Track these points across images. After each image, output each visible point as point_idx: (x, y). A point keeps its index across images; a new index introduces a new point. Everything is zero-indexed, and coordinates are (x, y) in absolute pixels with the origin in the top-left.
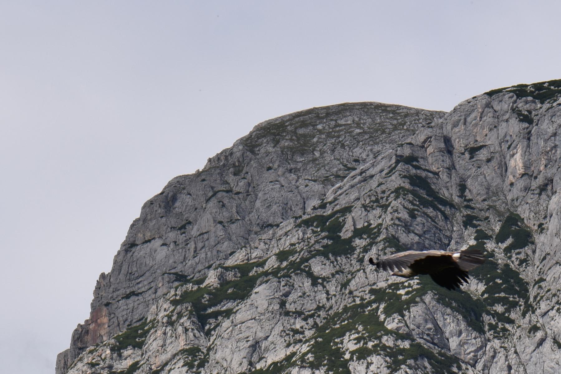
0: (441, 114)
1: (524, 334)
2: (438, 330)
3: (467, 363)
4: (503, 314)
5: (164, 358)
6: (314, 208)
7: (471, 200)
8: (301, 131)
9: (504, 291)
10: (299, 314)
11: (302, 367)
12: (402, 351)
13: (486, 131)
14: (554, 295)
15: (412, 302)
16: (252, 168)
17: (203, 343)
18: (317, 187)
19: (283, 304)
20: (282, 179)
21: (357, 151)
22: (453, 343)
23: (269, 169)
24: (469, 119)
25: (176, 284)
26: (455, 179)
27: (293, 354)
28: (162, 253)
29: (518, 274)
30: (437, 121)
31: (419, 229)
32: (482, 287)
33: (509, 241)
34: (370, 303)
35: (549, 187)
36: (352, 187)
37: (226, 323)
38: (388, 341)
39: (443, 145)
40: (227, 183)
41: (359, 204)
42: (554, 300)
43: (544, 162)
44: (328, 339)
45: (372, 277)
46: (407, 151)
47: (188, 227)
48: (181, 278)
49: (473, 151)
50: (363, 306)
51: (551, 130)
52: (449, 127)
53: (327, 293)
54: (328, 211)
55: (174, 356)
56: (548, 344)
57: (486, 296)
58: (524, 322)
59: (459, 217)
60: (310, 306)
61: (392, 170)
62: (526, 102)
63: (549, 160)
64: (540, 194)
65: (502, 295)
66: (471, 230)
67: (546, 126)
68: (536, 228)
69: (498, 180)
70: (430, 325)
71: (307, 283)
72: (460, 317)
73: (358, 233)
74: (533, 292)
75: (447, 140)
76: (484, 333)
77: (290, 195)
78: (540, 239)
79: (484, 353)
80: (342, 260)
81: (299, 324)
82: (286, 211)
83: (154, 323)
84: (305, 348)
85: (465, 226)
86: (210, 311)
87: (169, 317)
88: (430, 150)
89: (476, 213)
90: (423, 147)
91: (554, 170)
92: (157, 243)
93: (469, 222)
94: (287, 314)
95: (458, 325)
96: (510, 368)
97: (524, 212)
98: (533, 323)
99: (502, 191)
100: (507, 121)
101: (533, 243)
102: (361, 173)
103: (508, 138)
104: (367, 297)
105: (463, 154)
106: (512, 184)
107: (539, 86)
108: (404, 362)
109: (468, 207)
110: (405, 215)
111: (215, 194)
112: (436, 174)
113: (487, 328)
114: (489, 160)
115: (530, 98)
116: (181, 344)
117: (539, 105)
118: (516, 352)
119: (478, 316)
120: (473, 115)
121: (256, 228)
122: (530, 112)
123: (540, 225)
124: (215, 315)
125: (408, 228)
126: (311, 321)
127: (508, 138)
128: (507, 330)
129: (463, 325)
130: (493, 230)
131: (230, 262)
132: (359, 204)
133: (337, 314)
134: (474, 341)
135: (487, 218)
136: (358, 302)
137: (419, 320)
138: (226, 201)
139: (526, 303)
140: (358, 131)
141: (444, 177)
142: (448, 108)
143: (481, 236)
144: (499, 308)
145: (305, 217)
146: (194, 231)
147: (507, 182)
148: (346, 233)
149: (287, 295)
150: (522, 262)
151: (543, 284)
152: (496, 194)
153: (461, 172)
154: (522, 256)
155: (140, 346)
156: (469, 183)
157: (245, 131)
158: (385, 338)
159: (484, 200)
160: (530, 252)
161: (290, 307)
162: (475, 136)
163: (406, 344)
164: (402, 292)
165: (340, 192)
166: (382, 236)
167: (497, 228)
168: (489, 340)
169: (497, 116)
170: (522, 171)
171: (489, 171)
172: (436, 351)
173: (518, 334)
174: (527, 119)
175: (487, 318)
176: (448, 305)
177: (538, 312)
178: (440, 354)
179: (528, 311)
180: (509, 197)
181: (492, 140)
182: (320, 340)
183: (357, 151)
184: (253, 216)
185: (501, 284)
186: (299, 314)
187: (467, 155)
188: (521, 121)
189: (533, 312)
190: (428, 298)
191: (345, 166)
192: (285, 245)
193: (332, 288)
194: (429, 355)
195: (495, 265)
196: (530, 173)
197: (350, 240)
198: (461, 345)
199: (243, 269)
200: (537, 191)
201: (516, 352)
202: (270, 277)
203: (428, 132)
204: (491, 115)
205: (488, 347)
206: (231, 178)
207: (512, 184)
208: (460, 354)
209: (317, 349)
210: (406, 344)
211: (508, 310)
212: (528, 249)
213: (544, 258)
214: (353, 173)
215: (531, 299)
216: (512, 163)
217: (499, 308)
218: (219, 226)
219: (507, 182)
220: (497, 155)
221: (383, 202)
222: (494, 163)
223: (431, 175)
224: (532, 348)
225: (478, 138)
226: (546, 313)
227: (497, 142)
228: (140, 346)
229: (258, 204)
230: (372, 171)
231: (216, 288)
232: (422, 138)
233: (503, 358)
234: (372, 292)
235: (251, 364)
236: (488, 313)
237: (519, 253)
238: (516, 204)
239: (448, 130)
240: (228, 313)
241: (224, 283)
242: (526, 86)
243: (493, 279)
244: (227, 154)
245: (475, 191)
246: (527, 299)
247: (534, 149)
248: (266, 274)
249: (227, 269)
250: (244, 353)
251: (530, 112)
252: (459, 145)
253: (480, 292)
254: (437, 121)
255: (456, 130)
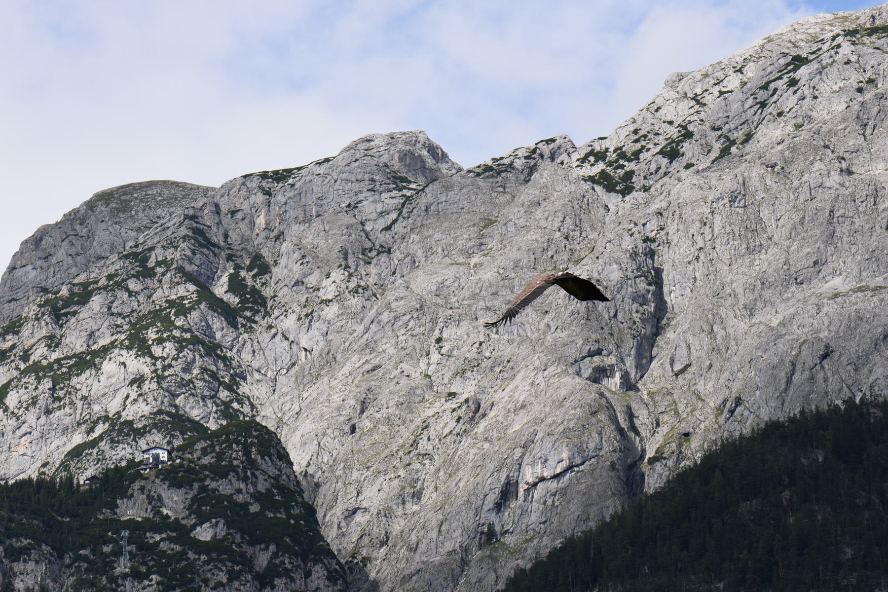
0: (213, 189)
1: (264, 330)
2: (209, 326)
3: (227, 348)
4: (251, 317)
5: (32, 341)
6: (131, 247)
7: (231, 244)
8: (123, 198)
9: (251, 302)
10: (119, 314)
11: (121, 349)
12: (185, 340)
13: (242, 200)
14: (283, 306)
15: (192, 308)
16: (91, 221)
17: (58, 332)
18: (133, 234)
19: (109, 308)
20: (110, 228)
21: (159, 212)
22: (218, 335)
23: (103, 221)
24: (231, 193)
25: (41, 294)
26: (221, 231)
27: (116, 340)
28: (33, 274)
29: (261, 292)
30: (210, 193)
31: (198, 262)
32: (237, 300)
33: (255, 271)
34: (165, 309)
35: (281, 237)
36: (156, 234)
37: (73, 320)
38: (177, 333)
39: (214, 209)
40: (75, 230)
41: (159, 245)
42: (283, 309)
43: (278, 221)
44: (138, 331)
45: (167, 292)
46: (191, 212)
47: (50, 258)
48: (45, 290)
49: (233, 213)
50: (161, 310)
51: (283, 201)
52: (218, 197)
53: (138, 302)
54: (140, 249)
55: (39, 340)
56: (279, 336)
57: (240, 305)
58: (264, 323)
59: (223, 255)
60: (127, 310)
61: (181, 224)
62: (268, 183)
63: (282, 220)
64: (275, 241)
65: (250, 305)
66: (231, 263)
67: (280, 198)
68: (272, 263)
69: (249, 232)
70: (203, 324)
71: (126, 295)
72: (223, 319)
73: (159, 264)
74: (270, 303)
75: (217, 206)
76: (238, 329)
77: (116, 238)
78: (275, 270)
79: (238, 342)
80: (148, 281)
81: (119, 321)
82: (113, 248)
83: (27, 319)
84: (123, 337)
85: (227, 261)
86: (63, 311)
87: (36, 315)
88: (206, 211)
89: (234, 252)
90: (201, 209)
91: (285, 226)
92: (30, 267)
93: (229, 258)
94: (112, 314)
95: (221, 323)
96: (254, 352)
97: (265, 252)
98: (269, 324)
99: (251, 239)
100: (255, 194)
101: (270, 272)
102: (161, 226)
103: (256, 205)
104: (164, 305)
105: (227, 214)
106: (258, 235)
107: (276, 173)
108: (186, 347)
109: (229, 248)
110: (188, 253)
111: (67, 236)
112: (209, 227)
113: (240, 326)
114: (243, 219)
115: (270, 180)
116: (44, 332)
117: (276, 185)
118: (258, 342)
119: (235, 318)
120: (233, 190)
121: (93, 259)
122: (270, 189)
123: (275, 261)
124: (66, 314)
125: (190, 261)
126: (127, 319)
127: (256, 205)
128: (253, 328)
129: (225, 324)
130: (245, 264)
131: (76, 281)
132: (159, 245)
133: (144, 315)
134: (231, 334)
135: (241, 256)
136: (158, 307)
137: (197, 320)
138: (74, 242)
139: (265, 310)
140: (160, 198)
141: (214, 229)
142: (217, 185)
143: (237, 267)
144: (248, 314)
145: (125, 253)
146: (53, 260)
147: (255, 233)
148: (151, 263)
149: (112, 302)
150: (263, 284)
151: (276, 299)
152: (247, 241)
153: (226, 226)
154: (263, 281)
155: (17, 333)
156: (230, 233)
157: (88, 196)
158: (174, 331)
159: (240, 244)
160: (268, 278)
161: (114, 310)
162: (235, 203)
163: (188, 336)
164: (186, 302)
165: (147, 237)
166: (174, 266)
167: (248, 263)
168: (241, 334)
169: (249, 191)
170: (264, 226)
171: (243, 226)
172: (207, 340)
173: (259, 330)
174: (268, 193)
175: (240, 320)
176: (215, 311)
177: (273, 316)
178: (209, 342)
179: (266, 315)
180: (256, 243)
181: (246, 206)
182: (133, 331)
183: (159, 212)
184: (92, 251)
185: (250, 298)
186: (119, 314)
187: (229, 216)
188: (264, 194)
189: (270, 317)
190: (202, 306)
191: (151, 221)
192: (112, 270)
193: (141, 298)
194: (202, 343)
195: (246, 286)
196: (269, 228)
197: (153, 268)
198: (223, 336)
199: (85, 285)
200: (274, 239)
201: (258, 342)
202: (102, 291)
203: (205, 200)
204: (245, 190)
205: (240, 338)
206: (78, 227)
207: (258, 235)
208: (222, 342)
209: (131, 337)
210: (188, 336)
211: (254, 315)
212: (267, 276)
213: (277, 282)
214: (156, 225)
215: (269, 308)
216: (258, 221)
217: (248, 314)
218: (70, 258)
219: (255, 233)
220: (249, 216)
221: (175, 244)
222: (246, 221)
223: (206, 227)
224: (269, 339)
225: (237, 205)
226: (277, 317)
227: (249, 208)
228: (17, 333)
229: (95, 244)
230: (168, 224)
231: (67, 297)
232: (201, 204)
233: (250, 345)
234: (167, 301)
235: (88, 346)
236: (241, 317)
237: (261, 279)
238: (260, 247)
239: (217, 199)
240: (74, 313)
241: (72, 294)
242: (268, 172)
243: (244, 295)
244: (76, 211)
245: (234, 239)
246: (266, 308)
247: (272, 213)
248: (99, 289)
249: (74, 285)
250: (84, 339)
251: (270, 189)
252: (224, 209)
253: (236, 303)
254: (210, 193)
255: (223, 199)
